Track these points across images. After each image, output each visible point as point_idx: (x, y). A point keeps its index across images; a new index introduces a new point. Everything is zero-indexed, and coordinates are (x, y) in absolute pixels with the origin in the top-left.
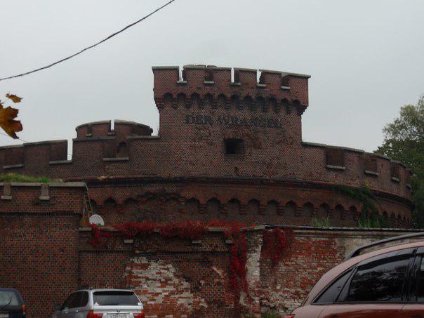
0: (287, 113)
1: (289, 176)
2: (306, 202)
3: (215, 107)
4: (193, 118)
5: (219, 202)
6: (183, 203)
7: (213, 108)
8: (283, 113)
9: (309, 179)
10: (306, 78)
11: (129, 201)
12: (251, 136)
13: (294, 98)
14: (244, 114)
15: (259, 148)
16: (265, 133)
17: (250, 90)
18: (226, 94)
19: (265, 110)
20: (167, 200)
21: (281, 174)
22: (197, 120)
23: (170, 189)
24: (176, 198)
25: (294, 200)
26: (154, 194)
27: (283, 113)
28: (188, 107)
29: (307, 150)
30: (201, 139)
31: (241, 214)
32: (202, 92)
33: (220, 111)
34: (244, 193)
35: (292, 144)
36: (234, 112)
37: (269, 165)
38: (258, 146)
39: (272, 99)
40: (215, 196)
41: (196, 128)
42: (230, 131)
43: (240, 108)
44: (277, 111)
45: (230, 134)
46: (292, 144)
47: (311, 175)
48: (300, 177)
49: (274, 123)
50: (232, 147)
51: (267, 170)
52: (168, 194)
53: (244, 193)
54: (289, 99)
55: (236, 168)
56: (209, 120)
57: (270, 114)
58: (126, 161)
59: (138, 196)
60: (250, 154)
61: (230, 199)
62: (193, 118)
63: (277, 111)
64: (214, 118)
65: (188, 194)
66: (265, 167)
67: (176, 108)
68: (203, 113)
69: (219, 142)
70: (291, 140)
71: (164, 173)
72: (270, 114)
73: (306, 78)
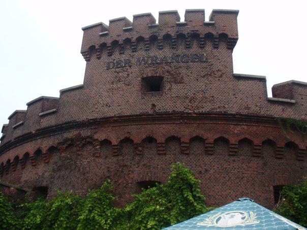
0: (215, 48)
1: (218, 110)
2: (242, 137)
3: (135, 50)
4: (114, 64)
5: (131, 141)
6: (98, 147)
7: (133, 52)
8: (209, 47)
9: (245, 112)
10: (235, 13)
11: (52, 149)
12: (172, 72)
13: (220, 32)
14: (167, 52)
15: (181, 83)
16: (188, 68)
17: (169, 29)
18: (144, 36)
19: (188, 47)
20: (84, 145)
21: (207, 108)
22: (118, 65)
23: (85, 133)
24: (88, 141)
25: (225, 136)
26: (72, 140)
27: (209, 47)
28: (110, 55)
29: (241, 82)
30: (119, 81)
31: (159, 154)
32: (121, 40)
33: (141, 53)
34: (161, 131)
35: (221, 76)
36: (155, 52)
37: (192, 99)
38: (178, 80)
40: (128, 135)
41: (115, 72)
42: (148, 69)
43: (161, 48)
44: (202, 47)
45: (149, 72)
46: (221, 76)
48: (233, 109)
49: (199, 59)
51: (190, 104)
52: (83, 139)
53: (161, 131)
54: (214, 33)
55: (154, 105)
57: (195, 49)
58: (54, 113)
59: (59, 143)
60: (170, 89)
61: (144, 137)
62: (114, 64)
63: (202, 47)
64: (133, 61)
65: (101, 136)
66: (187, 101)
67: (99, 58)
68: (124, 57)
69: (137, 82)
70: (220, 73)
71: (82, 117)
72: (195, 49)
73: (235, 13)
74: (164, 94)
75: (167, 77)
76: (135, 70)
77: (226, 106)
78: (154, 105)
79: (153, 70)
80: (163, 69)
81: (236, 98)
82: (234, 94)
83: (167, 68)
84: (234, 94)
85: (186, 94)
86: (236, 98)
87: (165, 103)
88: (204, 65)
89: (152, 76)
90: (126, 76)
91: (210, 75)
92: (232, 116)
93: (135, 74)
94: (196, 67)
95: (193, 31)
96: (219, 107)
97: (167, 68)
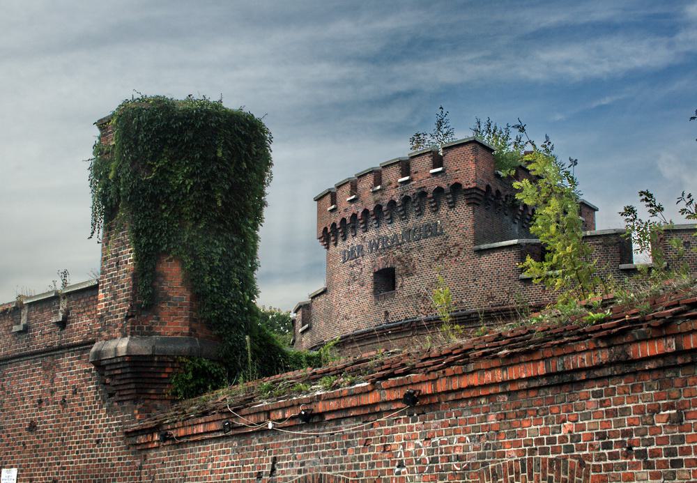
0: (451, 208)
3: (366, 230)
7: (364, 232)
8: (444, 210)
13: (452, 182)
16: (420, 248)
19: (420, 213)
29: (485, 257)
33: (372, 234)
35: (458, 255)
39: (422, 194)
41: (351, 266)
42: (379, 258)
44: (436, 210)
46: (458, 255)
47: (491, 298)
49: (432, 231)
50: (386, 280)
51: (422, 306)
54: (444, 186)
56: (360, 248)
66: (420, 302)
69: (369, 279)
70: (455, 251)
72: (428, 217)
74: (396, 295)
75: (398, 267)
76: (366, 261)
77: (464, 300)
78: (387, 313)
79: (384, 259)
80: (394, 256)
81: (477, 285)
82: (475, 280)
83: (398, 253)
84: (475, 280)
85: (418, 291)
86: (477, 285)
87: (400, 310)
88: (437, 239)
89: (383, 270)
90: (359, 271)
91: (445, 255)
92: (466, 317)
93: (368, 264)
94: (429, 243)
95: (420, 188)
96: (455, 305)
97: (398, 253)
